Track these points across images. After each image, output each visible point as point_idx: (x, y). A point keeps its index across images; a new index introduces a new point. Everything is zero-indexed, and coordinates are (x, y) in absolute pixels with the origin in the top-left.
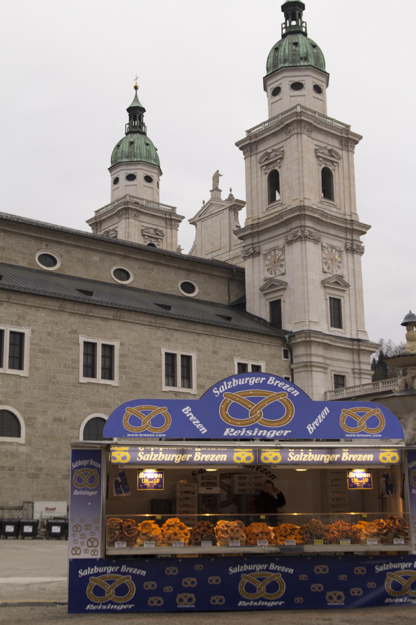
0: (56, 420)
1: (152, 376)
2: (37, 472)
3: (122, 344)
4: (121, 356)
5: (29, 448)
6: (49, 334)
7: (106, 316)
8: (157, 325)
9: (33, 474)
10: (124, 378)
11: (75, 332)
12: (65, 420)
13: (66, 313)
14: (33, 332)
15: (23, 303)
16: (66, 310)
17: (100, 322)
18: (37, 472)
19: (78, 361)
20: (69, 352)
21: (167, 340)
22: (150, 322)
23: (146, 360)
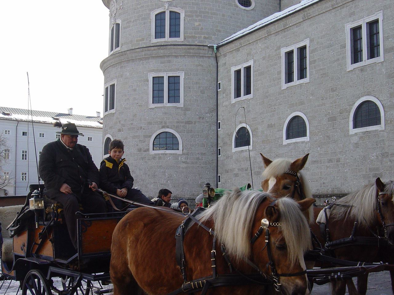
0: (270, 126)
1: (338, 60)
2: (259, 170)
3: (311, 41)
4: (312, 52)
5: (255, 152)
6: (264, 58)
7: (298, 22)
8: (340, 5)
9: (258, 172)
10: (314, 72)
11: (279, 48)
12: (274, 125)
13: (273, 35)
14: (255, 62)
15: (248, 43)
16: (272, 33)
17: (295, 29)
18: (259, 170)
19: (279, 73)
20: (276, 67)
21: (352, 14)
22: (332, 6)
23: (331, 46)
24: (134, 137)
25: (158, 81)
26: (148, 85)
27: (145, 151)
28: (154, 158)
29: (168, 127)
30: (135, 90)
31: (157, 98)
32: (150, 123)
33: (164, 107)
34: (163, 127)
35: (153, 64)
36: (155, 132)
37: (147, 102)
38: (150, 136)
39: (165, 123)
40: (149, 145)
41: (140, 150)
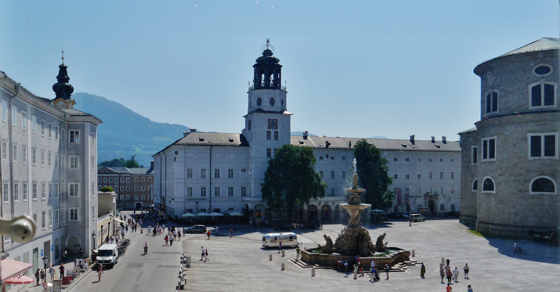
24: (514, 181)
25: (536, 141)
26: (527, 143)
27: (525, 192)
28: (533, 197)
29: (545, 175)
30: (515, 146)
31: (536, 151)
32: (529, 171)
33: (542, 160)
34: (540, 175)
35: (531, 126)
36: (534, 177)
37: (526, 156)
38: (529, 181)
39: (543, 172)
40: (528, 187)
41: (520, 191)
